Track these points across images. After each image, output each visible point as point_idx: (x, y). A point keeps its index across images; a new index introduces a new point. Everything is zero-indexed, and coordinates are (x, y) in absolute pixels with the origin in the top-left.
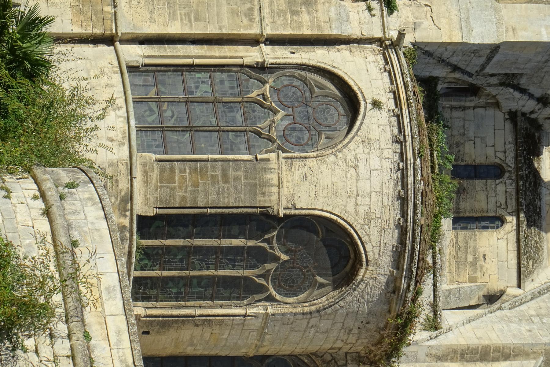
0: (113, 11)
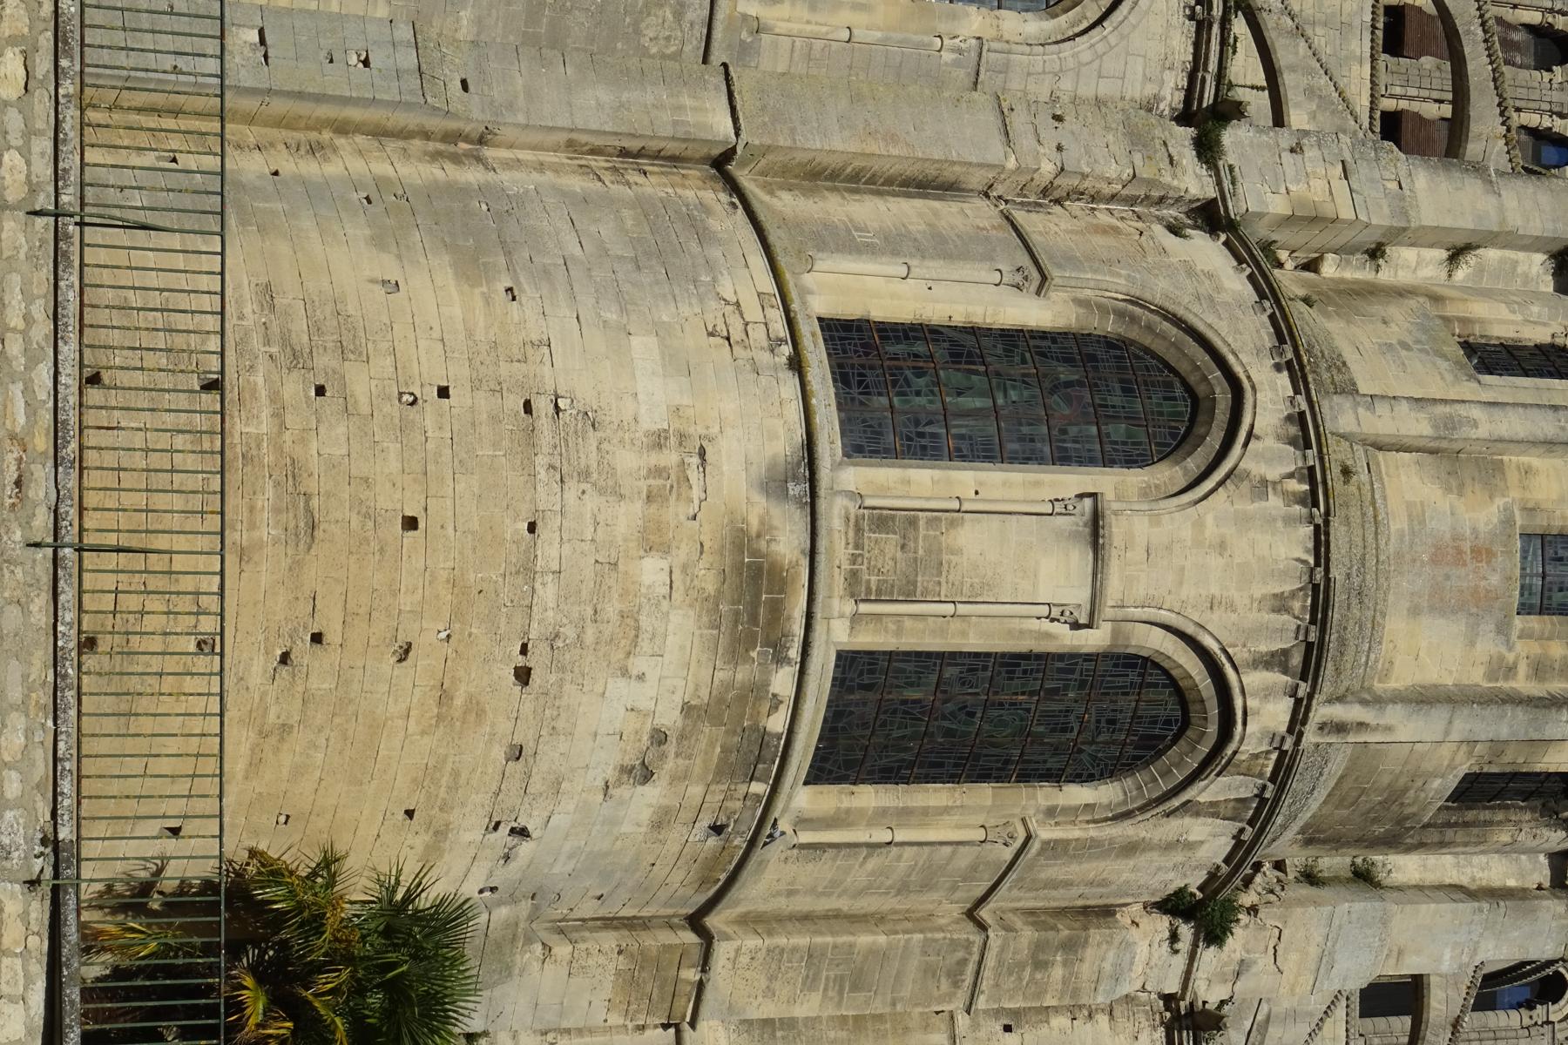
0: (697, 978)
